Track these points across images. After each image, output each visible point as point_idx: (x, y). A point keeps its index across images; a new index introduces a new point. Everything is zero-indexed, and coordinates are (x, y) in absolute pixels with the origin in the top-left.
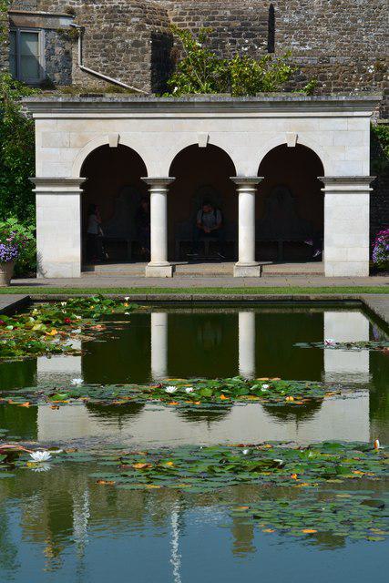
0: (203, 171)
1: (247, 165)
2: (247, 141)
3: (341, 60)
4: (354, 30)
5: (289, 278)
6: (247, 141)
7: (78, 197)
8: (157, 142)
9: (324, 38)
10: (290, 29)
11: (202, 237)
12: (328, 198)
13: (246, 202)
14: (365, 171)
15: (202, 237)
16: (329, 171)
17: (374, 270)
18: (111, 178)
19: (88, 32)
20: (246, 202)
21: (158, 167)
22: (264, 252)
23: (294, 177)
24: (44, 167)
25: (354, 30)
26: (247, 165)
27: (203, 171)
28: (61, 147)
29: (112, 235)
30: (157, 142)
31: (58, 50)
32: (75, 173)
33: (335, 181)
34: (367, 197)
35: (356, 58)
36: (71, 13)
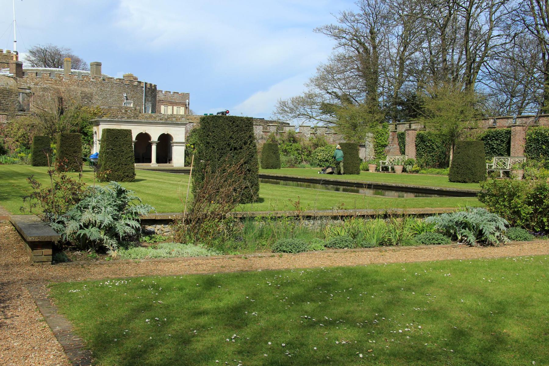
1: (155, 138)
2: (155, 133)
3: (115, 108)
4: (106, 98)
6: (155, 133)
9: (97, 100)
13: (154, 148)
14: (184, 141)
16: (174, 140)
17: (185, 166)
19: (35, 94)
20: (154, 148)
22: (158, 161)
23: (165, 141)
25: (106, 98)
26: (155, 138)
31: (25, 99)
33: (177, 143)
35: (119, 107)
36: (30, 88)
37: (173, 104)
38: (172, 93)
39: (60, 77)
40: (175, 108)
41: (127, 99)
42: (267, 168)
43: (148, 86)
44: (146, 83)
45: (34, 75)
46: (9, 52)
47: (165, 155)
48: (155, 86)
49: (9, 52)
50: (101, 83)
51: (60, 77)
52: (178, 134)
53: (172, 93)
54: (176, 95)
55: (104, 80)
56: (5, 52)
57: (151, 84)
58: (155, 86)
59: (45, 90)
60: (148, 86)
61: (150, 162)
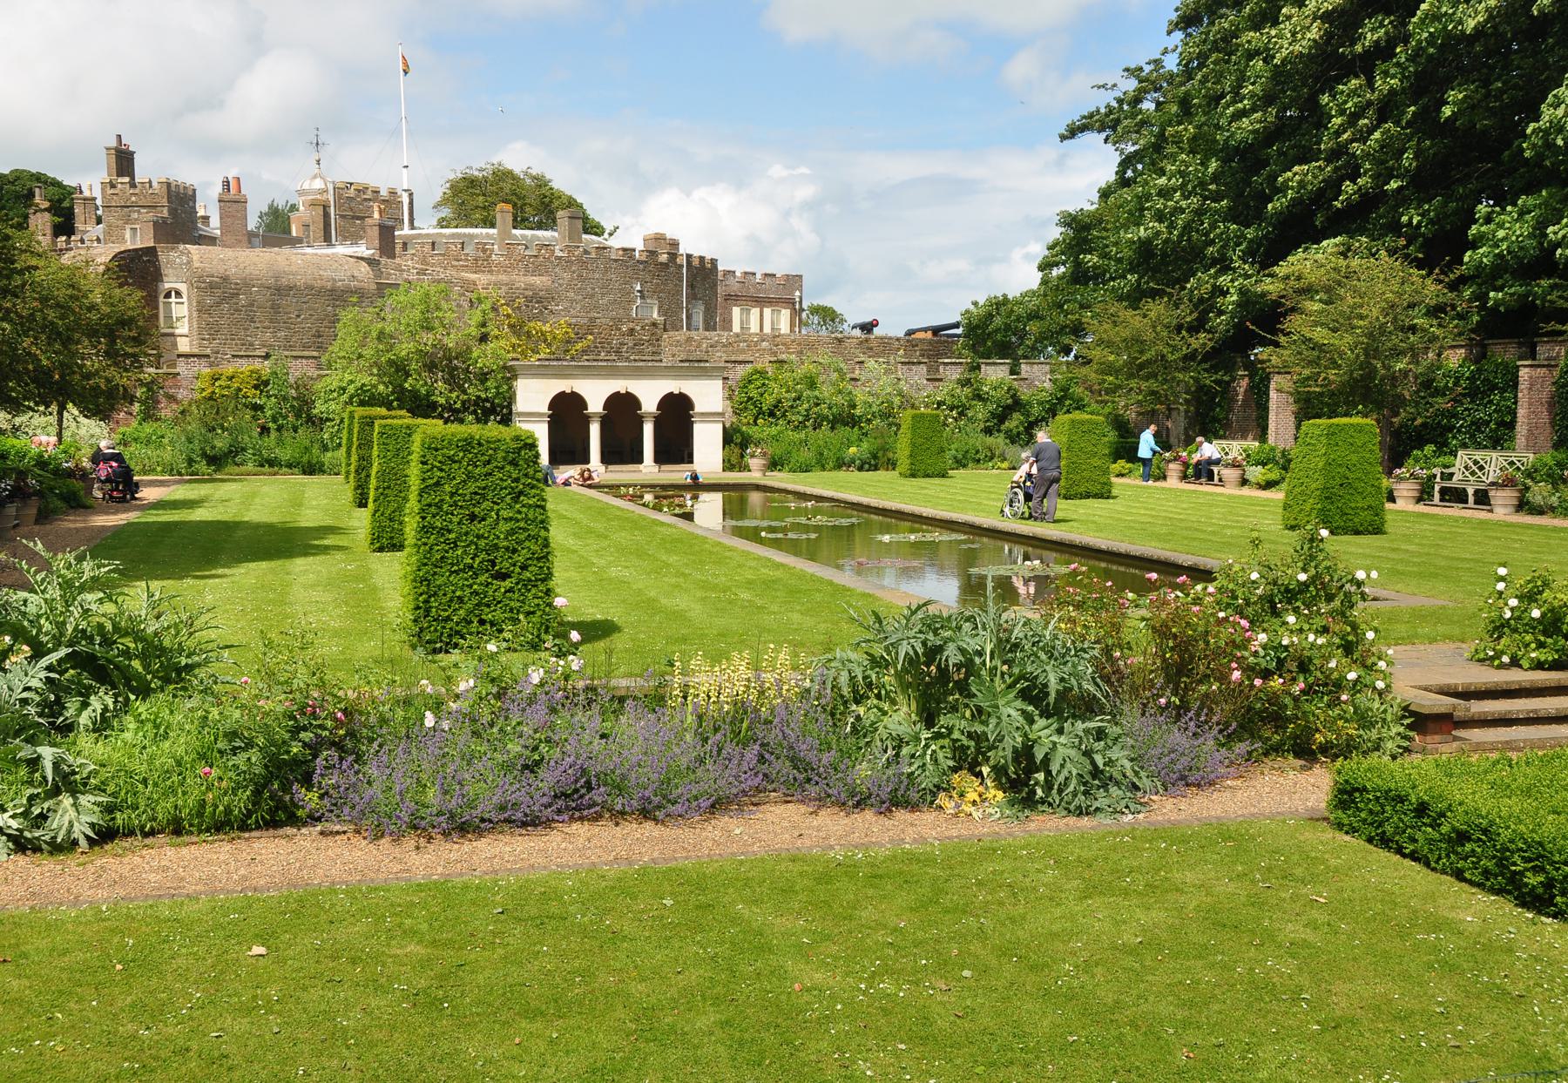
0: (622, 408)
1: (649, 404)
2: (650, 394)
4: (592, 296)
5: (677, 474)
7: (546, 426)
8: (595, 393)
9: (572, 301)
12: (696, 427)
16: (698, 409)
21: (595, 405)
22: (660, 458)
23: (677, 412)
24: (522, 404)
25: (592, 296)
26: (649, 404)
27: (622, 408)
28: (533, 397)
30: (595, 393)
32: (545, 409)
33: (703, 414)
37: (761, 302)
38: (758, 276)
39: (484, 251)
40: (767, 311)
41: (642, 297)
42: (913, 476)
43: (696, 263)
44: (689, 256)
45: (428, 248)
46: (393, 193)
47: (675, 446)
48: (714, 262)
49: (393, 193)
50: (579, 260)
51: (484, 251)
52: (707, 395)
53: (758, 276)
54: (768, 280)
55: (586, 252)
56: (384, 193)
57: (702, 258)
58: (714, 262)
60: (696, 263)
61: (640, 461)
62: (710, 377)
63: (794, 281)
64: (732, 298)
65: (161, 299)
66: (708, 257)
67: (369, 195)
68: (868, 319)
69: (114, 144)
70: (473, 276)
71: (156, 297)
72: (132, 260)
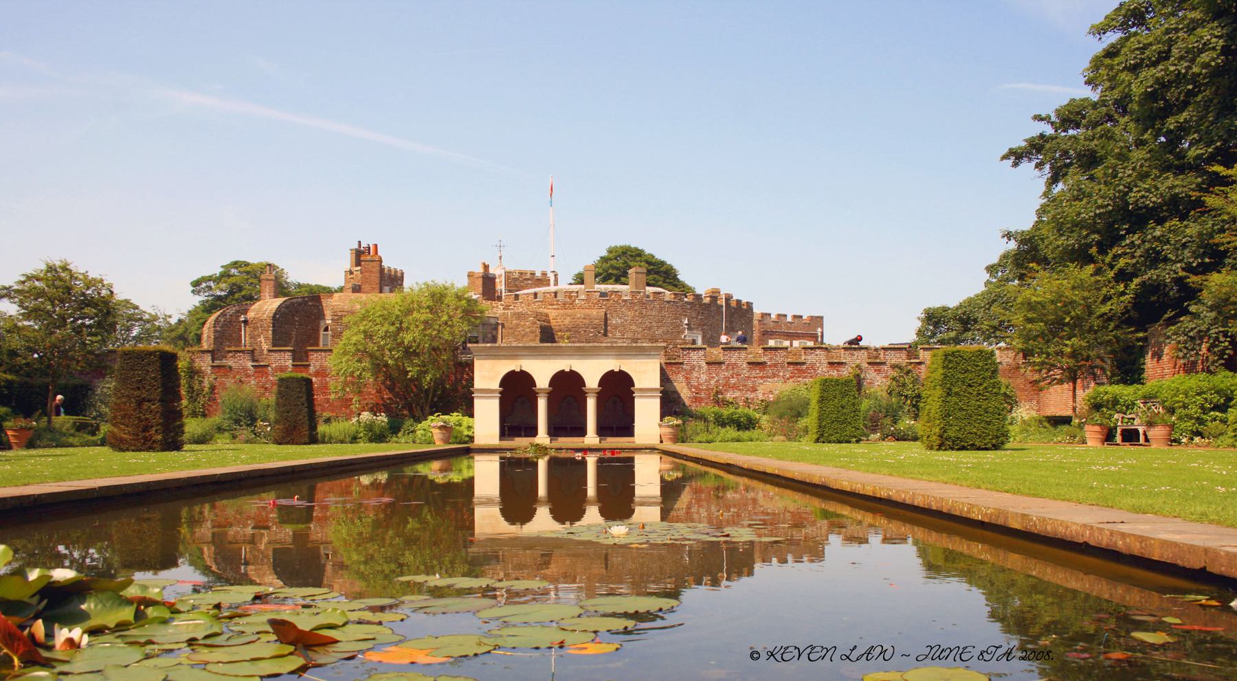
0: (568, 384)
2: (592, 371)
4: (650, 328)
6: (592, 371)
8: (542, 371)
9: (634, 332)
10: (616, 327)
11: (567, 422)
12: (639, 403)
15: (567, 422)
16: (638, 385)
18: (516, 390)
23: (618, 390)
24: (479, 383)
25: (650, 328)
27: (568, 384)
28: (488, 374)
29: (516, 421)
30: (542, 371)
32: (495, 385)
34: (658, 401)
38: (789, 319)
39: (570, 297)
43: (733, 304)
46: (544, 274)
48: (749, 305)
49: (544, 274)
51: (570, 297)
52: (645, 373)
53: (789, 319)
54: (797, 320)
56: (538, 274)
57: (739, 302)
58: (749, 305)
59: (519, 316)
60: (733, 304)
62: (649, 356)
63: (818, 321)
64: (767, 334)
65: (322, 332)
66: (744, 301)
67: (528, 276)
68: (854, 336)
69: (356, 246)
70: (546, 311)
71: (318, 331)
72: (300, 304)
